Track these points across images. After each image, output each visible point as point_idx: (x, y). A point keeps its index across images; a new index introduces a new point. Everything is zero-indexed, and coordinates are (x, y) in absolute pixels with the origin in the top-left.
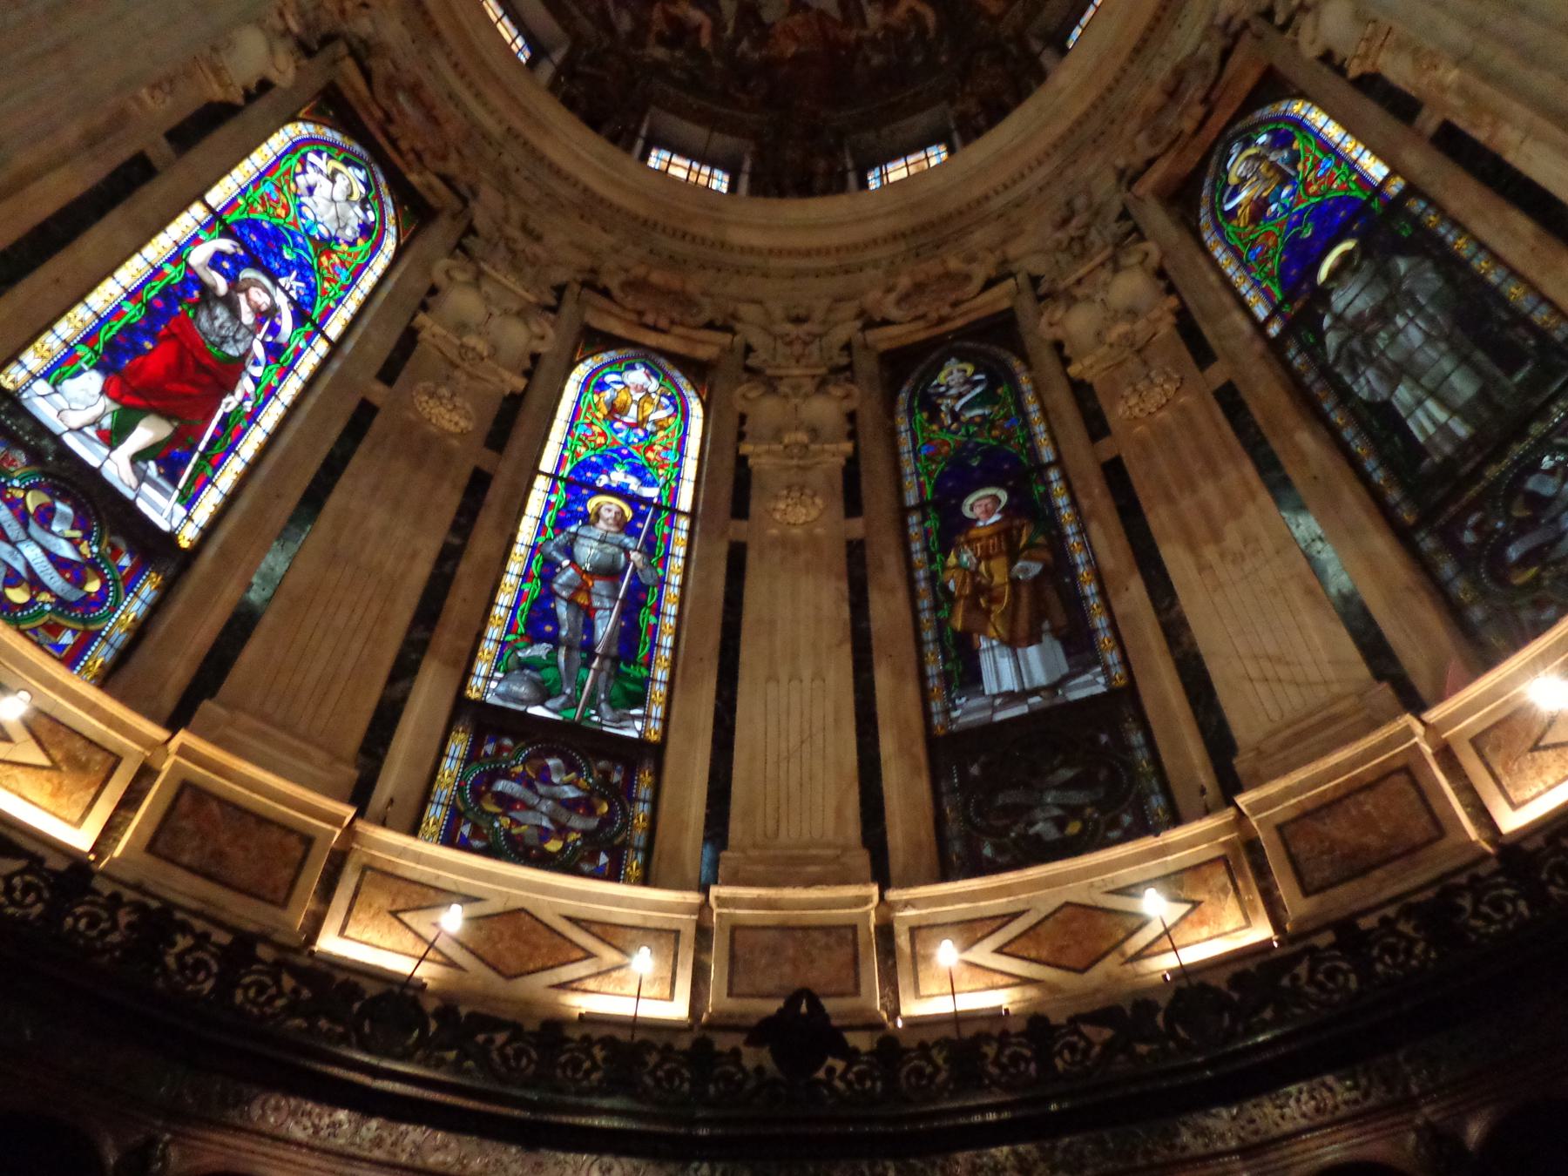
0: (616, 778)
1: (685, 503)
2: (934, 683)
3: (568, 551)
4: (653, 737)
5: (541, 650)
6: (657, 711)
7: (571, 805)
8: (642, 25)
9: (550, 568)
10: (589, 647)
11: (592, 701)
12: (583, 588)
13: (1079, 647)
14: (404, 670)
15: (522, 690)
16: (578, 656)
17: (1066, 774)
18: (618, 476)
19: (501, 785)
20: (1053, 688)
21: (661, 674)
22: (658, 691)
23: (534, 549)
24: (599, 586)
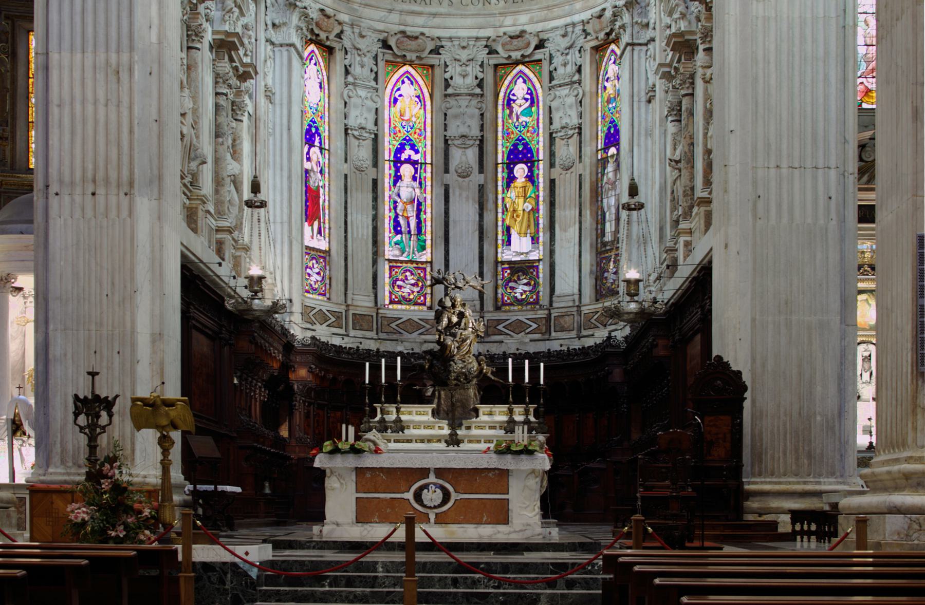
0: (422, 275)
1: (428, 161)
2: (500, 242)
3: (399, 195)
4: (429, 260)
5: (399, 236)
6: (429, 250)
7: (413, 285)
9: (395, 202)
10: (409, 232)
11: (414, 253)
12: (405, 210)
13: (535, 240)
14: (375, 262)
15: (397, 252)
16: (408, 236)
17: (525, 281)
18: (408, 153)
19: (399, 283)
20: (527, 253)
21: (429, 237)
22: (429, 243)
23: (390, 196)
24: (409, 207)
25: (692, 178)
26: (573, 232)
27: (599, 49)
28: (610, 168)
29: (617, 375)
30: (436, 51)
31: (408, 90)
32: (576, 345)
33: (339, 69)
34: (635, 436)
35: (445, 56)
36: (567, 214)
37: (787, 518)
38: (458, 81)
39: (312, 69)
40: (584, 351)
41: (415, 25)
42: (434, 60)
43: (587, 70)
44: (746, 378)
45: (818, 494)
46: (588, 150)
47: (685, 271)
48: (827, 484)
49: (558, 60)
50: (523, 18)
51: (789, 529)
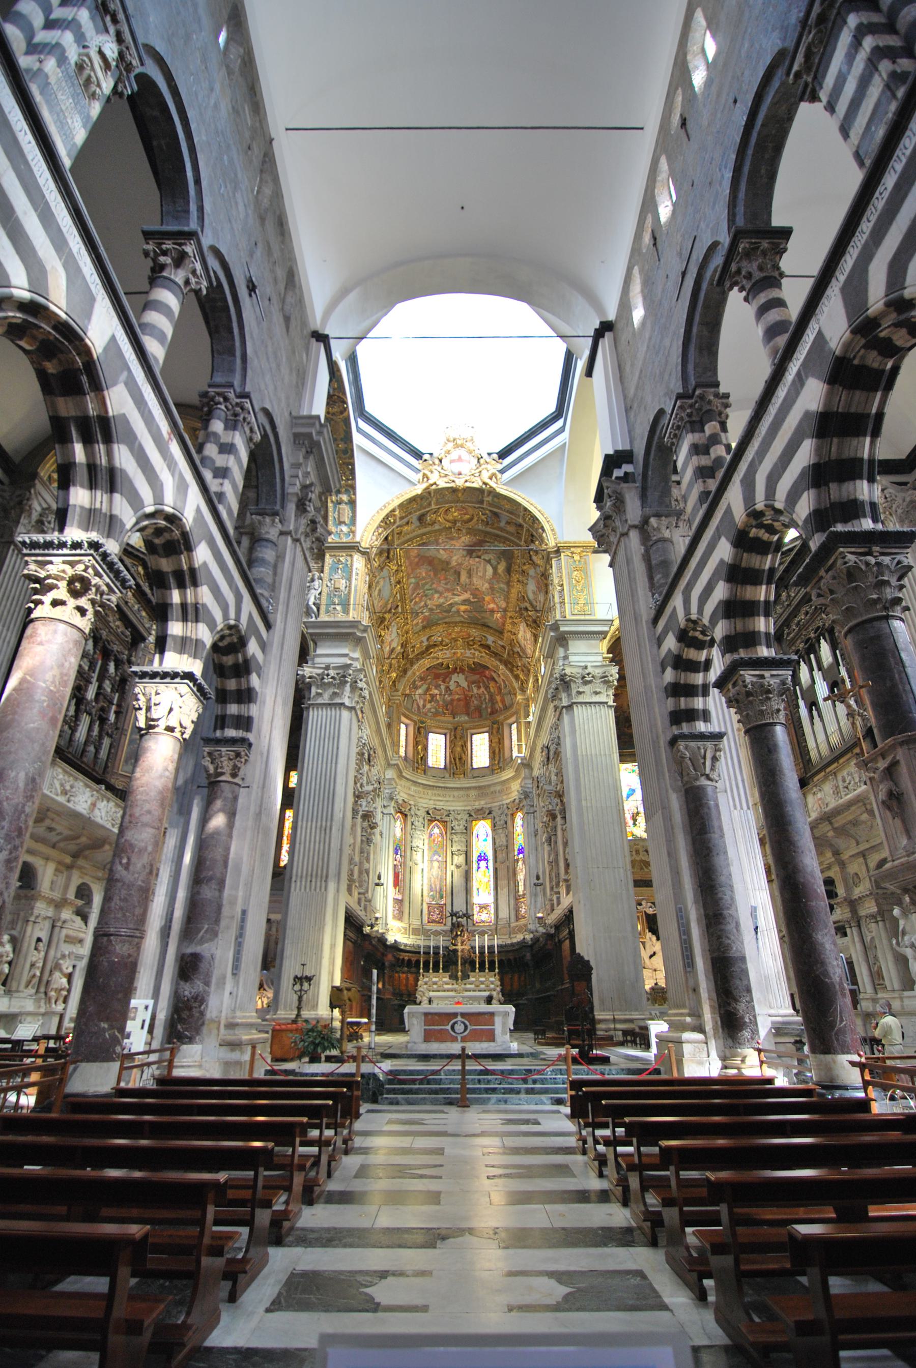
8: (425, 701)
25: (558, 869)
26: (506, 890)
27: (513, 815)
28: (520, 863)
29: (528, 956)
30: (448, 816)
31: (436, 831)
32: (509, 942)
33: (409, 823)
34: (538, 985)
35: (451, 817)
36: (503, 883)
37: (620, 1033)
38: (456, 828)
39: (398, 823)
40: (512, 945)
41: (440, 805)
42: (447, 819)
43: (509, 823)
44: (592, 964)
45: (631, 1021)
46: (511, 855)
47: (559, 912)
48: (635, 1015)
49: (497, 819)
50: (483, 802)
51: (621, 1039)
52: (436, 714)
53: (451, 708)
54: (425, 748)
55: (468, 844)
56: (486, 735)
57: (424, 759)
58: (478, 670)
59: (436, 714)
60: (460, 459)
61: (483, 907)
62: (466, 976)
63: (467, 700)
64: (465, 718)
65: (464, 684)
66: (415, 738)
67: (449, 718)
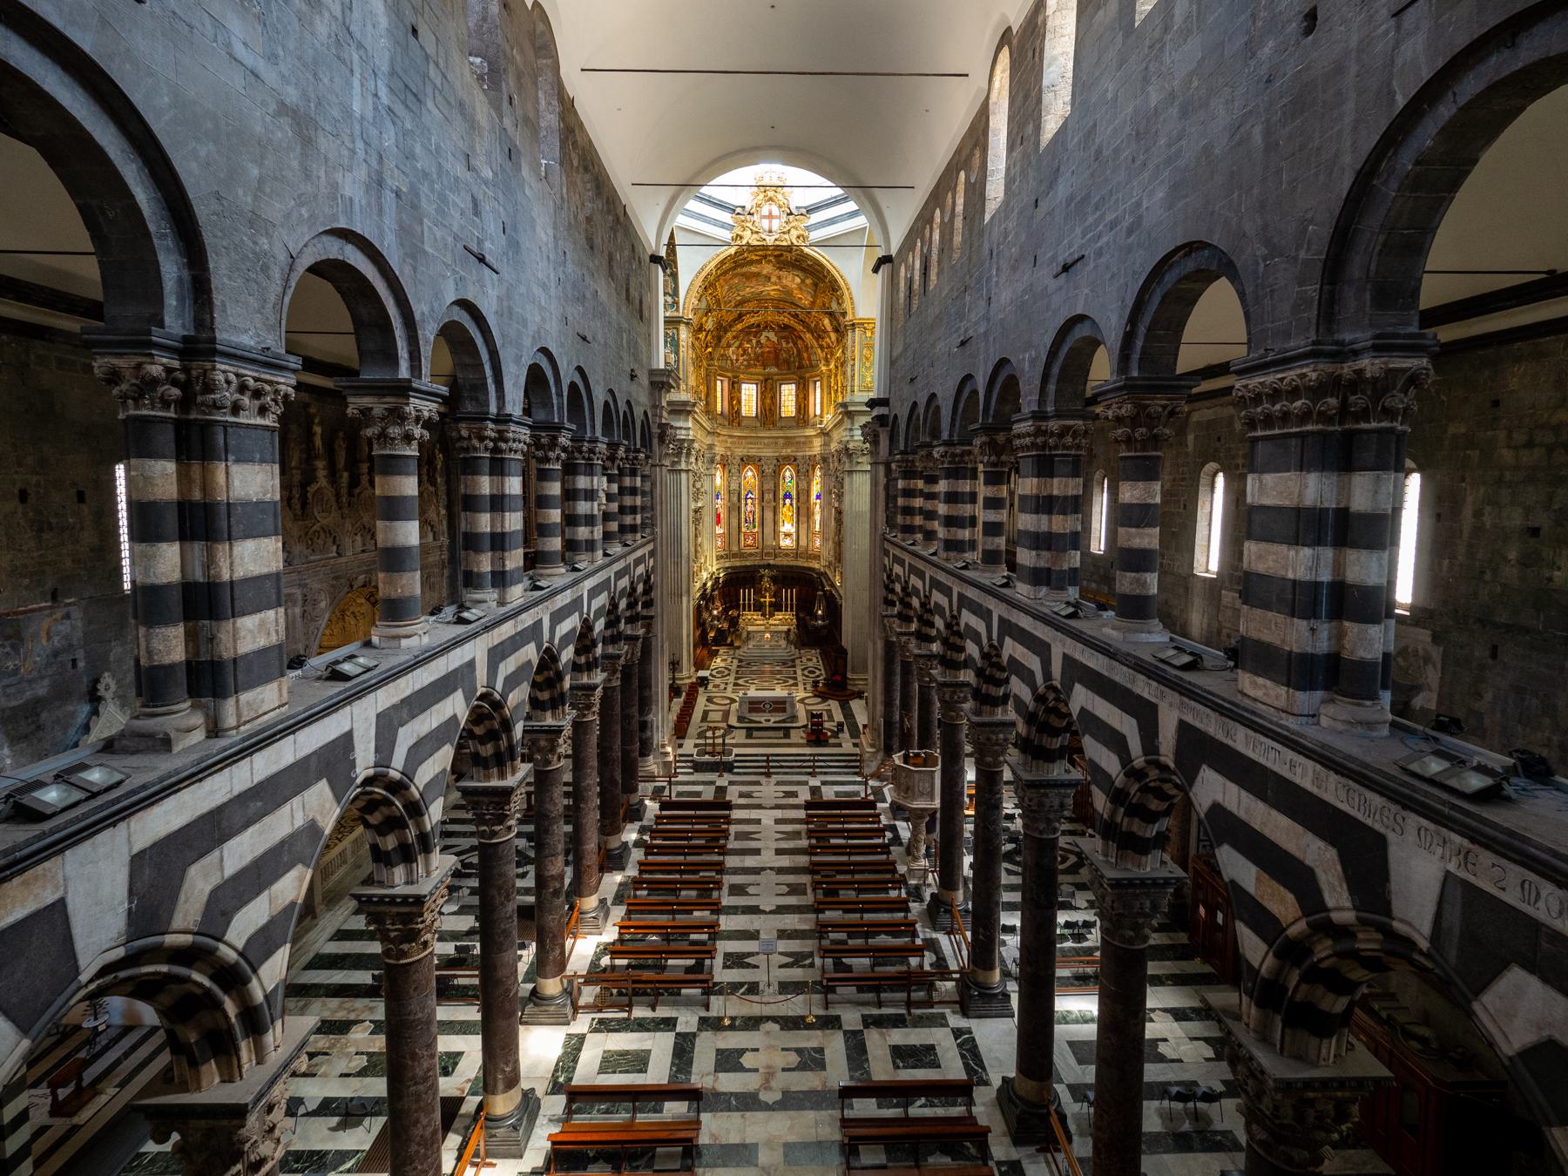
52: (749, 366)
53: (761, 360)
54: (739, 402)
55: (776, 486)
56: (793, 387)
57: (738, 412)
58: (786, 327)
59: (749, 366)
60: (770, 216)
61: (787, 535)
62: (772, 615)
63: (776, 352)
64: (774, 370)
65: (775, 339)
66: (730, 393)
67: (759, 370)
